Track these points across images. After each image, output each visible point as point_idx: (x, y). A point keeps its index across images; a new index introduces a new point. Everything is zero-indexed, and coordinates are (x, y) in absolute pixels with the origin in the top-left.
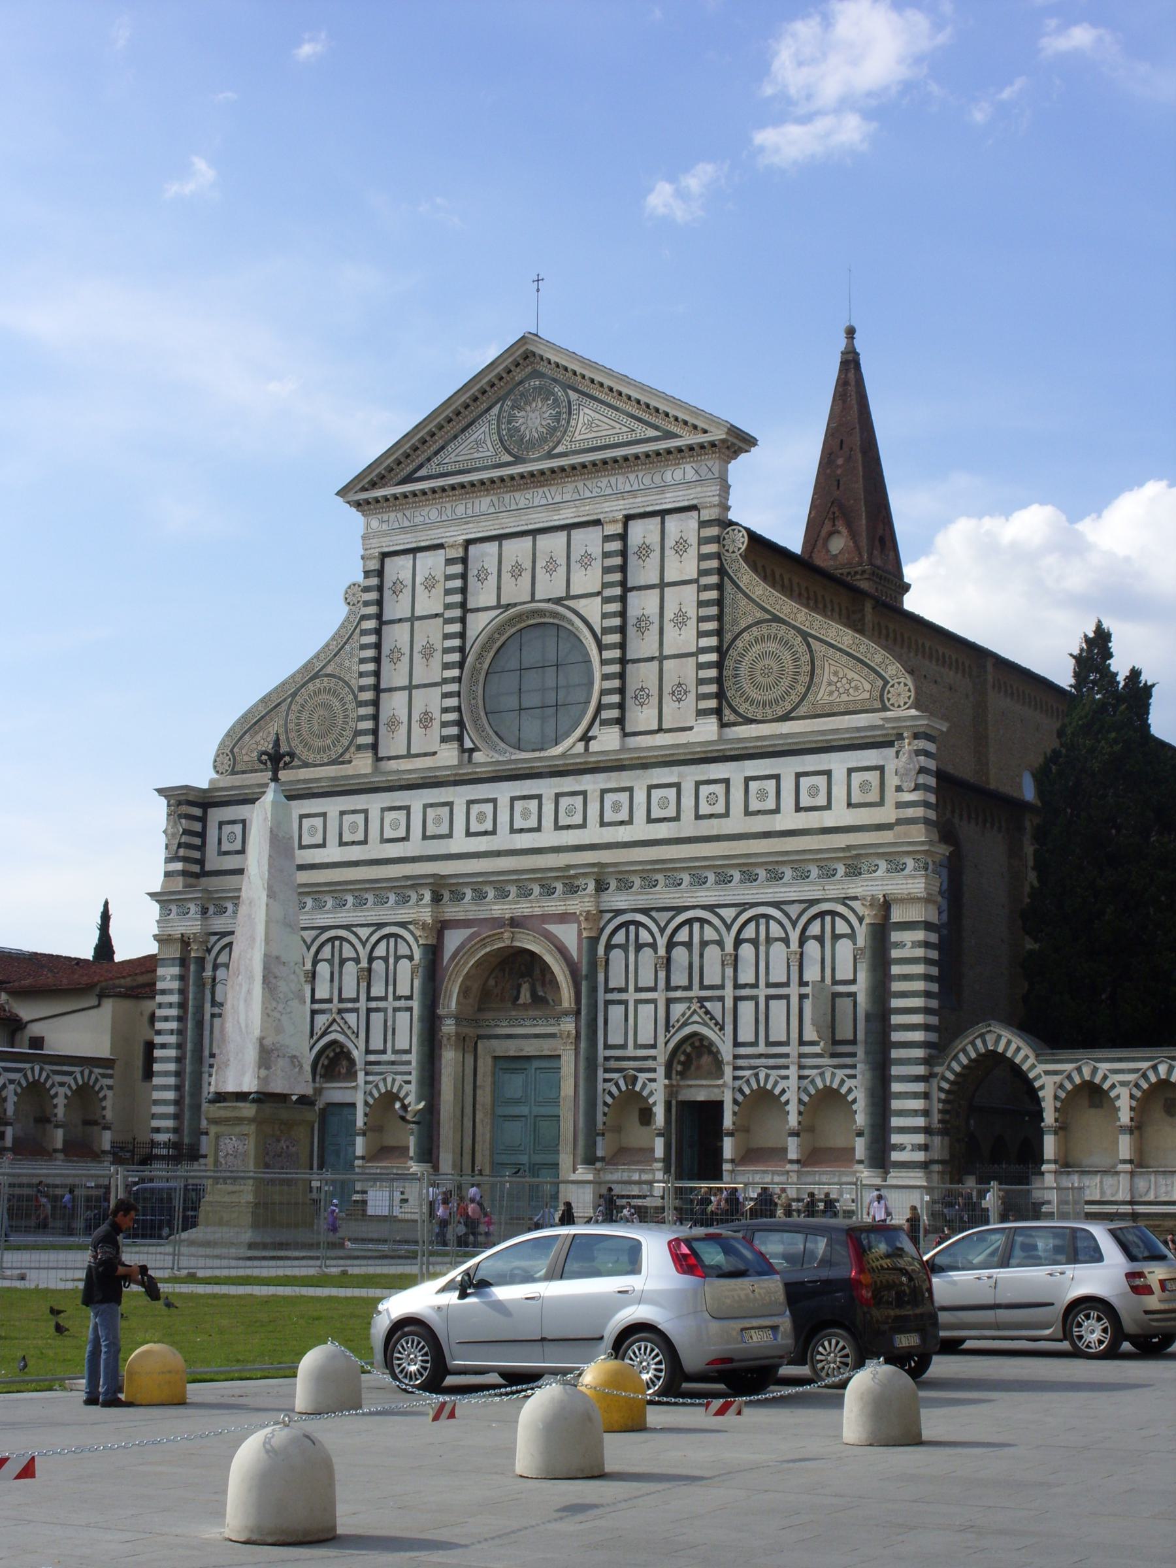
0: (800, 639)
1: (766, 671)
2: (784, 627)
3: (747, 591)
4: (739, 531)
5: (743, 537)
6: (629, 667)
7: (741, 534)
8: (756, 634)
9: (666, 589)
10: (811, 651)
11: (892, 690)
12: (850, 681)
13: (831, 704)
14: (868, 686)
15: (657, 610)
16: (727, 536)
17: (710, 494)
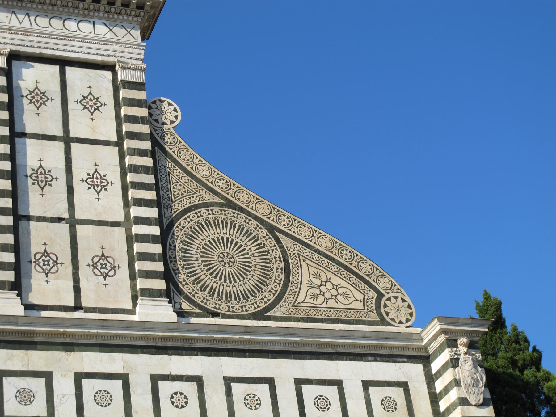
0: (265, 231)
1: (226, 260)
2: (242, 215)
3: (189, 168)
4: (170, 104)
5: (175, 110)
6: (22, 224)
7: (172, 108)
8: (206, 216)
9: (73, 145)
10: (282, 247)
11: (387, 303)
12: (337, 287)
13: (317, 307)
14: (360, 297)
15: (62, 165)
16: (153, 106)
17: (134, 56)
